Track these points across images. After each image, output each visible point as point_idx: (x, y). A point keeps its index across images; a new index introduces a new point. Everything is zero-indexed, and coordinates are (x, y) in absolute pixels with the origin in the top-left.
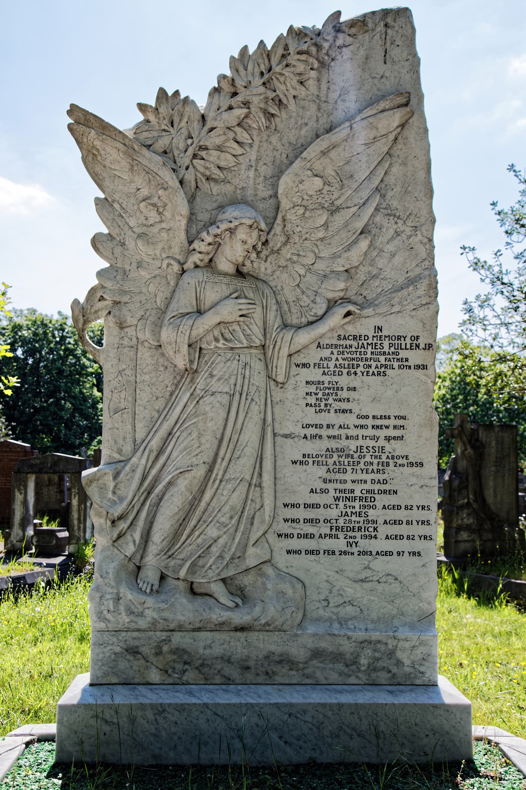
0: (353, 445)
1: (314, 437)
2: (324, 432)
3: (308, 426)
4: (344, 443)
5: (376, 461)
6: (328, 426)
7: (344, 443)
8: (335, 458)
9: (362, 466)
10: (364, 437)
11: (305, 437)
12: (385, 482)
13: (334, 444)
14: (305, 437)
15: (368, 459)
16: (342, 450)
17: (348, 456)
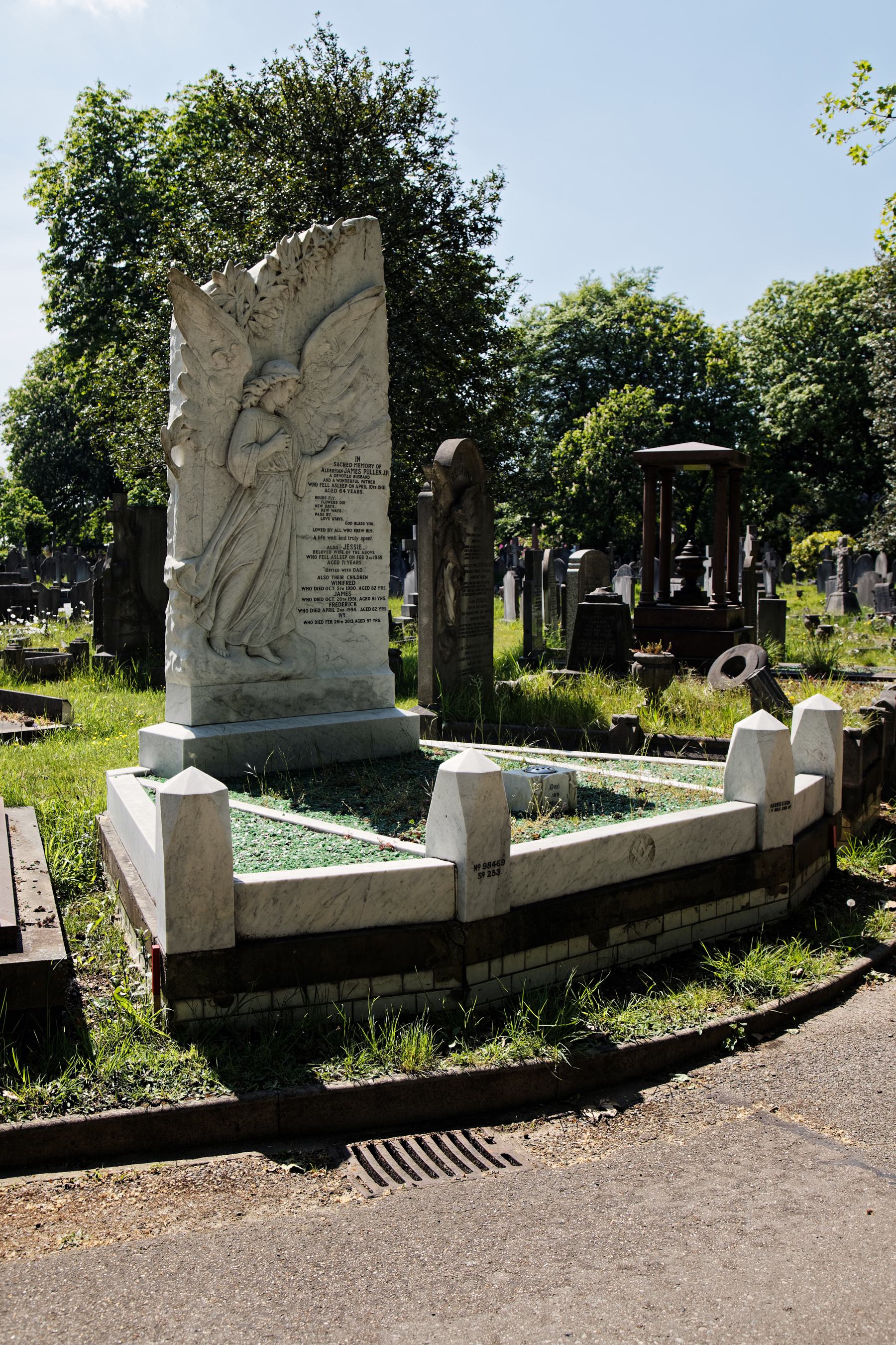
0: (343, 543)
1: (321, 538)
2: (326, 534)
3: (316, 530)
4: (338, 542)
5: (356, 555)
6: (329, 530)
7: (338, 542)
8: (333, 553)
9: (348, 559)
10: (350, 538)
11: (315, 538)
12: (361, 570)
13: (331, 543)
14: (315, 538)
15: (351, 554)
16: (336, 547)
17: (340, 552)
